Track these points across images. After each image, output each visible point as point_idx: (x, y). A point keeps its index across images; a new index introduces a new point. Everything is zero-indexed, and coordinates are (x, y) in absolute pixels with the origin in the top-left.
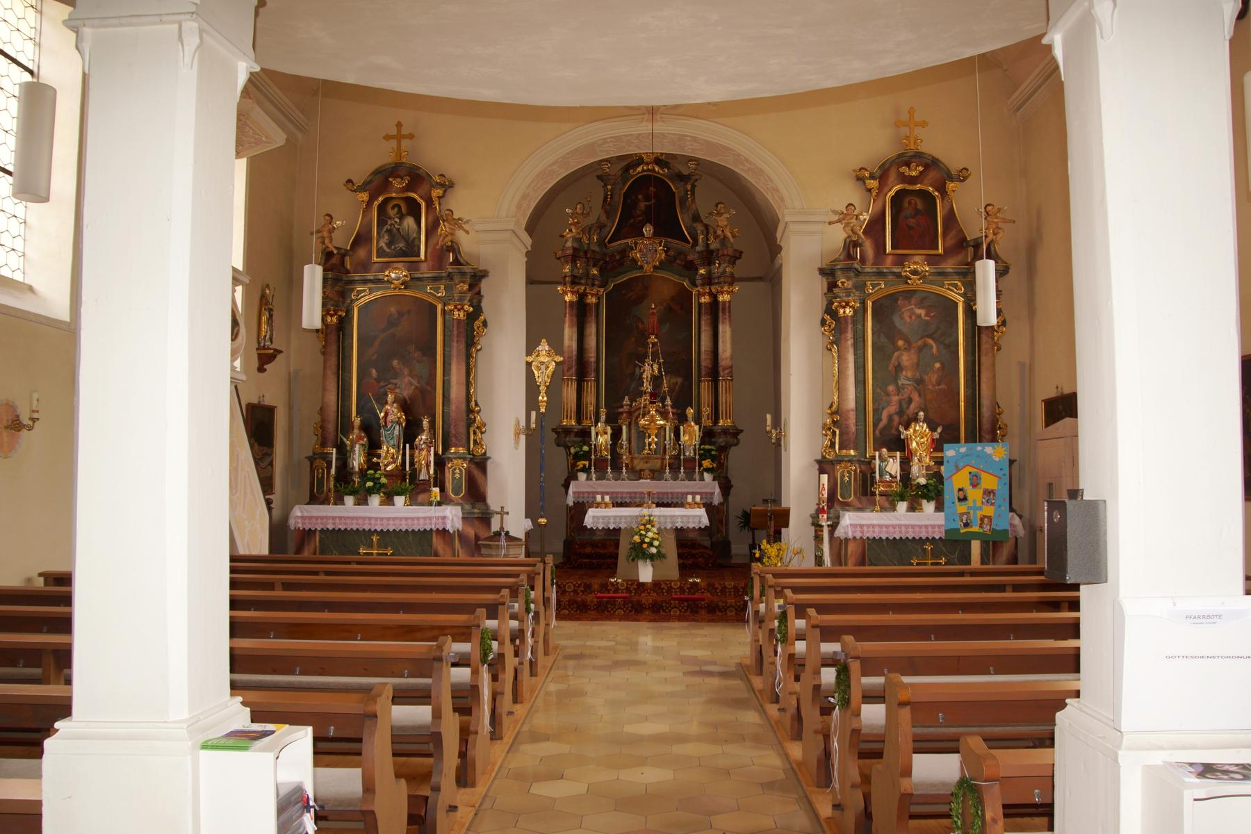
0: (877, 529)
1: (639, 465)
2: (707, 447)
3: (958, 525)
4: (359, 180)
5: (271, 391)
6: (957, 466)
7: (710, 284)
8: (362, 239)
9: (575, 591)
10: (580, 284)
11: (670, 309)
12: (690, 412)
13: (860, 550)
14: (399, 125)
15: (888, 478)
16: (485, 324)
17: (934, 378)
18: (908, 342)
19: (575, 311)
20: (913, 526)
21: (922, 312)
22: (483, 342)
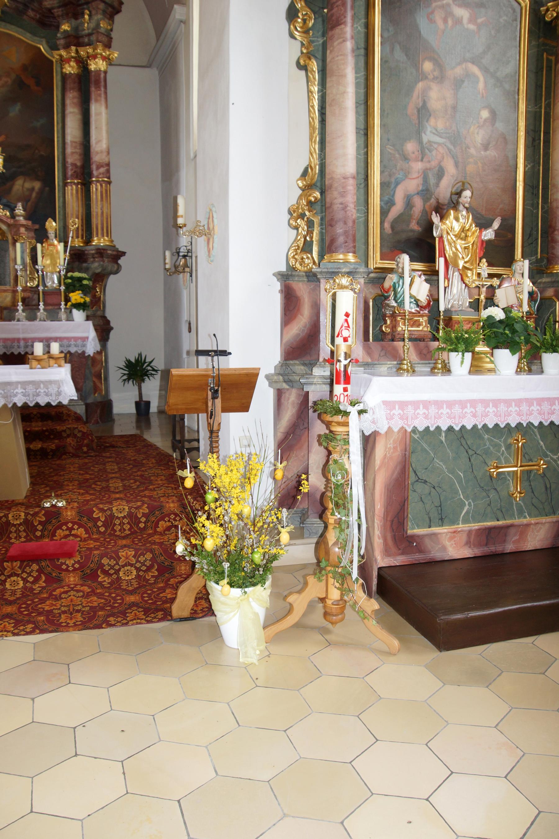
0: (433, 410)
2: (77, 274)
7: (79, 44)
11: (20, 84)
12: (52, 225)
13: (398, 453)
15: (414, 309)
20: (496, 403)
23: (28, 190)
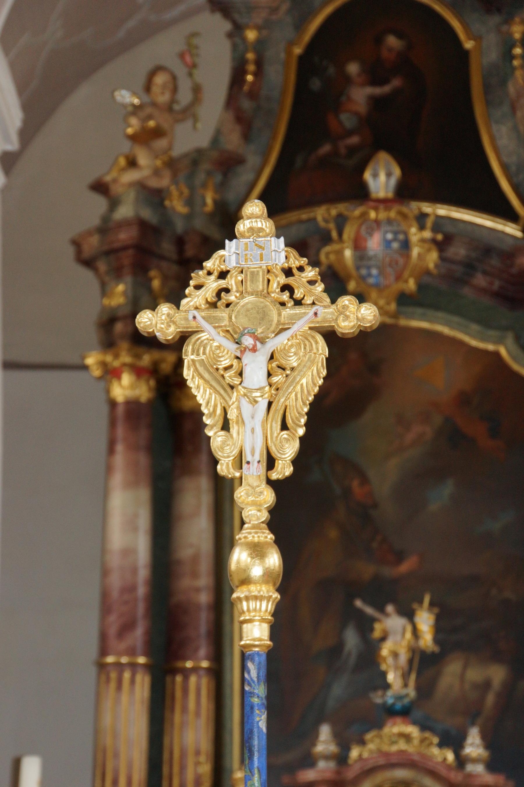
19: (143, 434)
23: (475, 686)
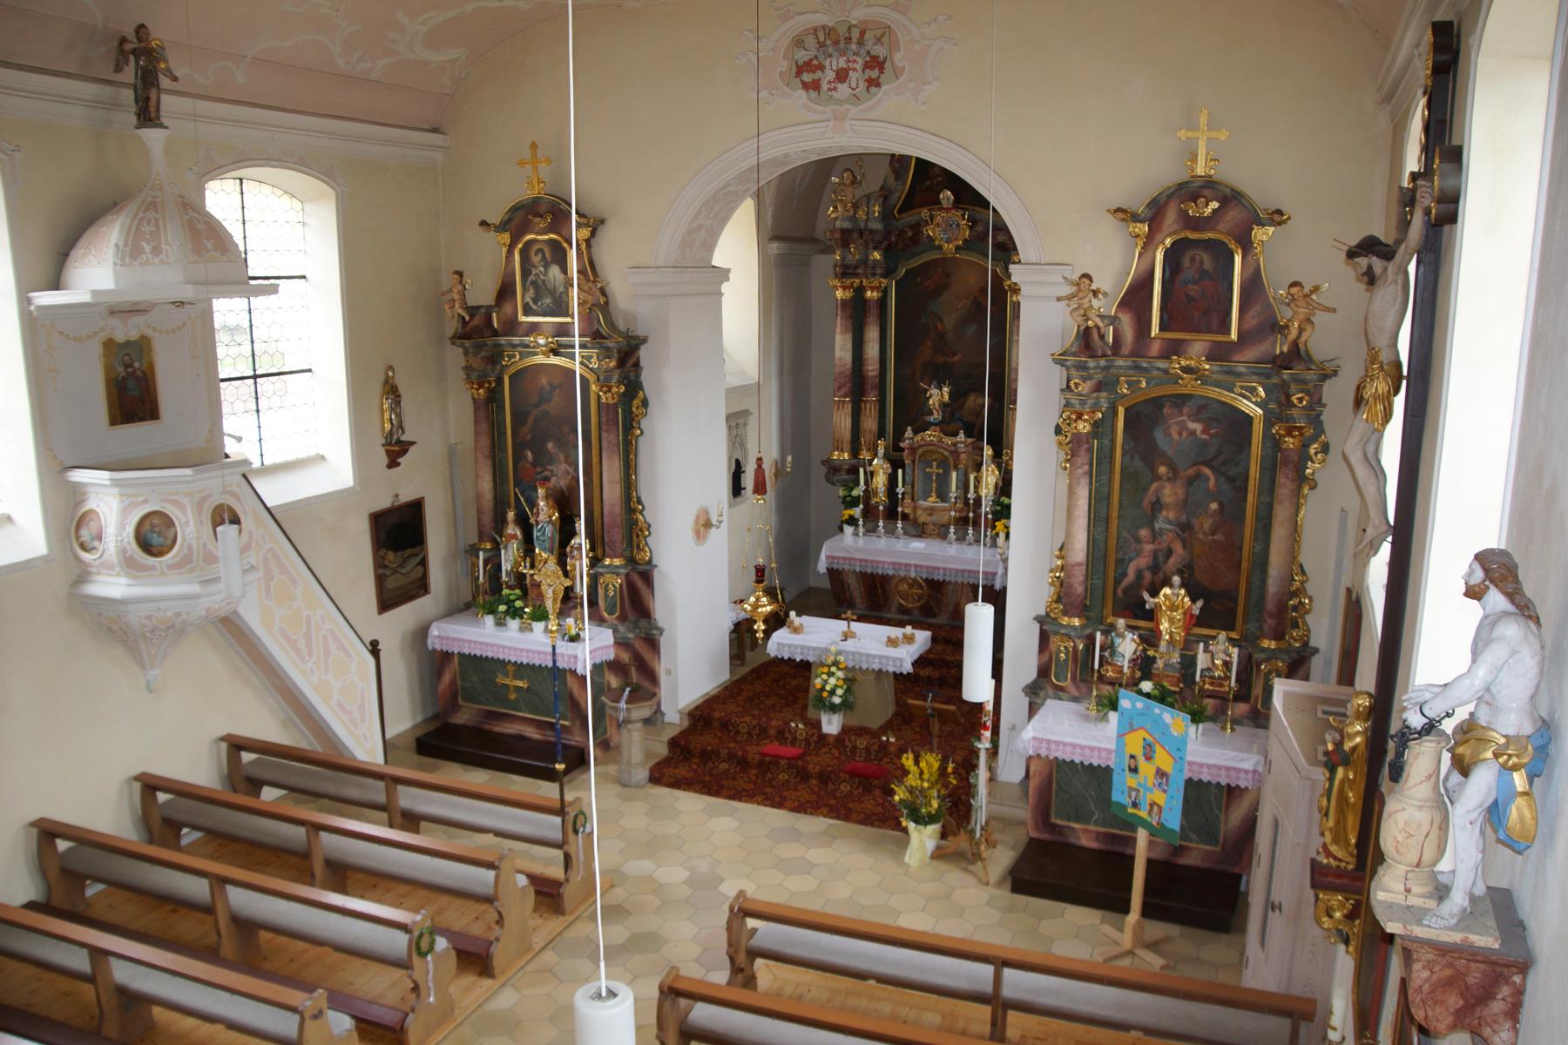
0: (1069, 749)
1: (923, 517)
3: (1126, 801)
4: (495, 219)
5: (415, 480)
6: (1131, 724)
8: (505, 291)
9: (749, 733)
10: (856, 275)
13: (1046, 771)
14: (534, 146)
16: (645, 403)
17: (1207, 524)
18: (1173, 469)
21: (1197, 427)
22: (644, 423)
